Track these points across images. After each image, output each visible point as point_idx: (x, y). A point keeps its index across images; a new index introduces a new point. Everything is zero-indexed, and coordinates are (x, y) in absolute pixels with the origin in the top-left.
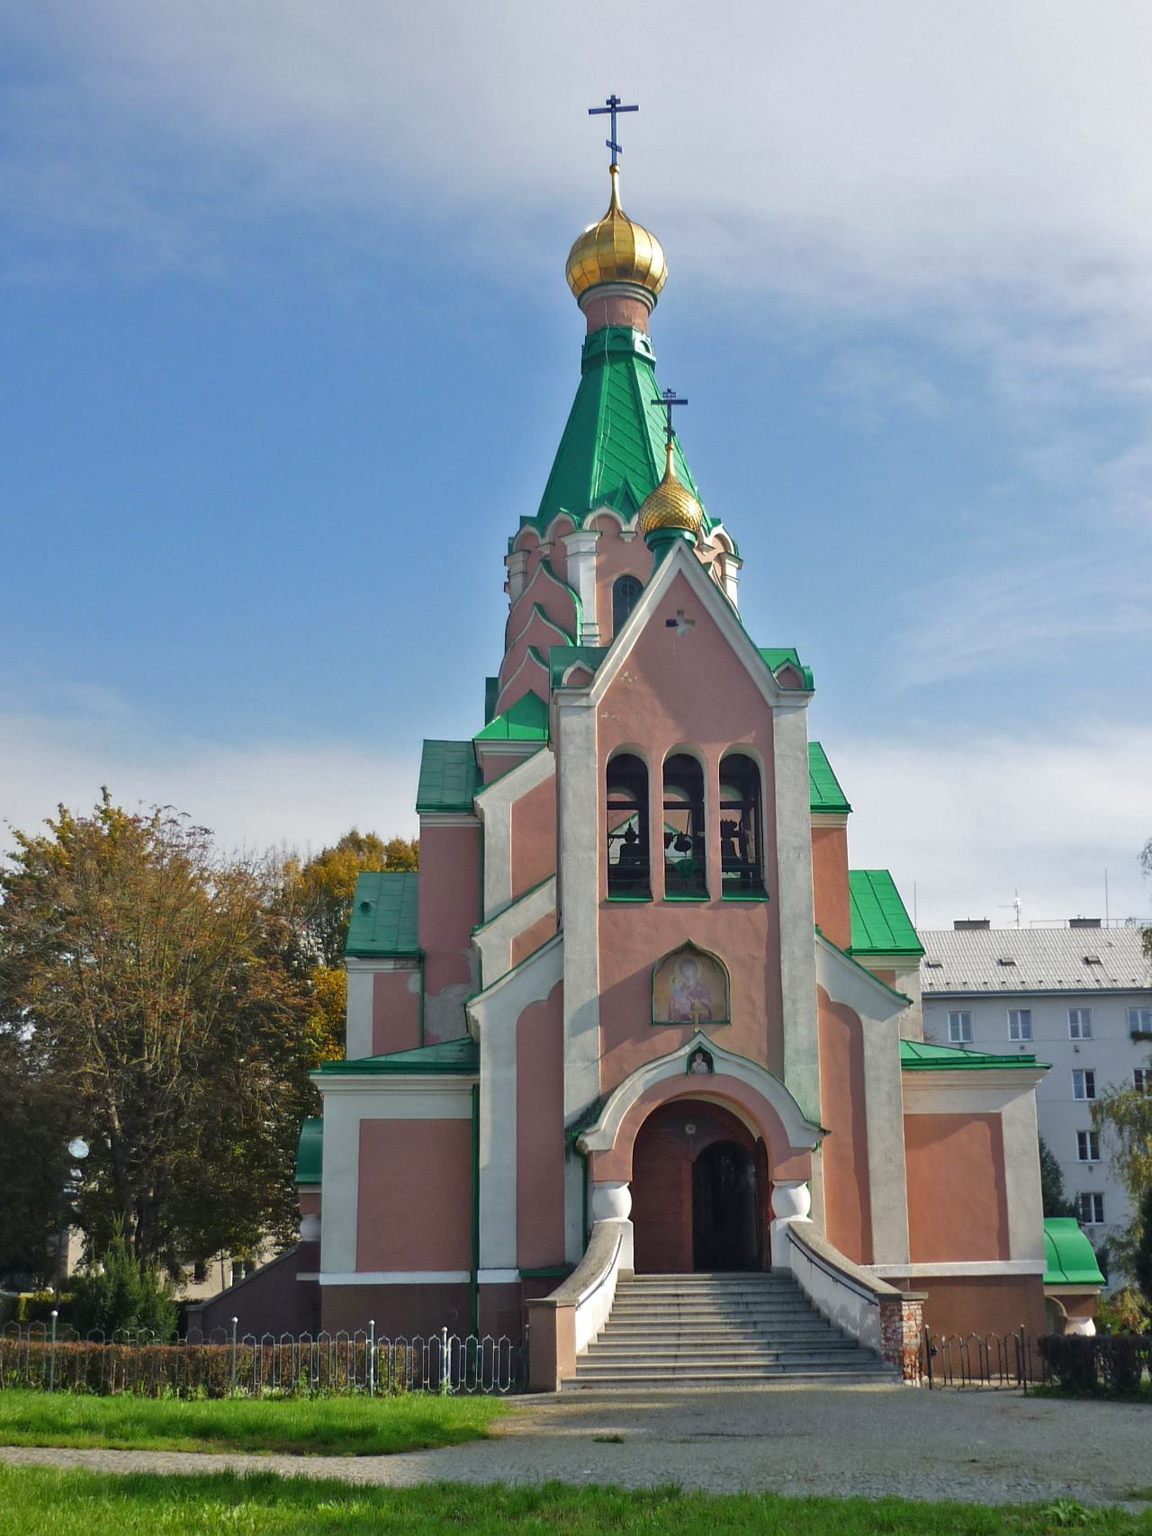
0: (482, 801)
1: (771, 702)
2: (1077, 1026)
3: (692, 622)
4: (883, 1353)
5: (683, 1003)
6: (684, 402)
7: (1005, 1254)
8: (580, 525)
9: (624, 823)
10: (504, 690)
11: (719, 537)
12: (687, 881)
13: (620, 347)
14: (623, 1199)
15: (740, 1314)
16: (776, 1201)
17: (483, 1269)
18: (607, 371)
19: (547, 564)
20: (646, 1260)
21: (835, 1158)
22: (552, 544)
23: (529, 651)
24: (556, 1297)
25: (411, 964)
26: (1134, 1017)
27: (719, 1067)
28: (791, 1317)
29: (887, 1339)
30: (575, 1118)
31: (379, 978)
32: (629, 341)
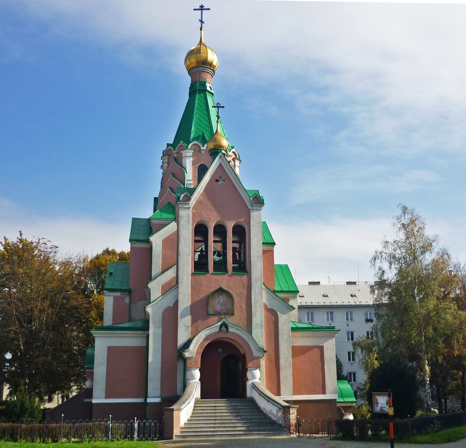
0: (152, 239)
1: (250, 208)
2: (348, 317)
3: (224, 180)
4: (284, 425)
5: (218, 308)
6: (223, 107)
7: (324, 392)
8: (187, 147)
9: (200, 247)
10: (160, 201)
11: (233, 152)
12: (221, 267)
13: (201, 88)
14: (197, 374)
15: (236, 412)
16: (249, 375)
17: (149, 397)
18: (197, 96)
19: (176, 159)
20: (205, 394)
21: (269, 361)
22: (177, 153)
23: (169, 188)
24: (174, 407)
25: (126, 293)
26: (366, 314)
27: (230, 330)
28: (253, 414)
29: (285, 421)
30: (181, 346)
31: (115, 298)
32: (205, 86)
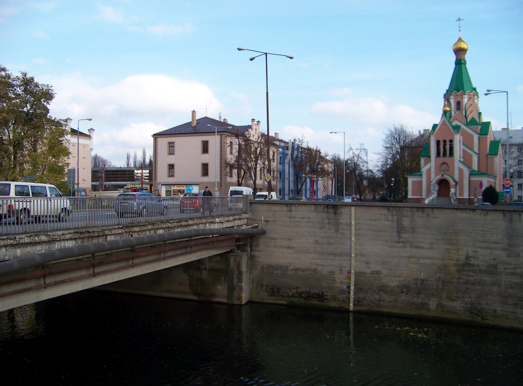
1: (454, 134)
3: (445, 125)
5: (444, 169)
8: (451, 94)
12: (445, 155)
27: (445, 176)
31: (425, 160)
